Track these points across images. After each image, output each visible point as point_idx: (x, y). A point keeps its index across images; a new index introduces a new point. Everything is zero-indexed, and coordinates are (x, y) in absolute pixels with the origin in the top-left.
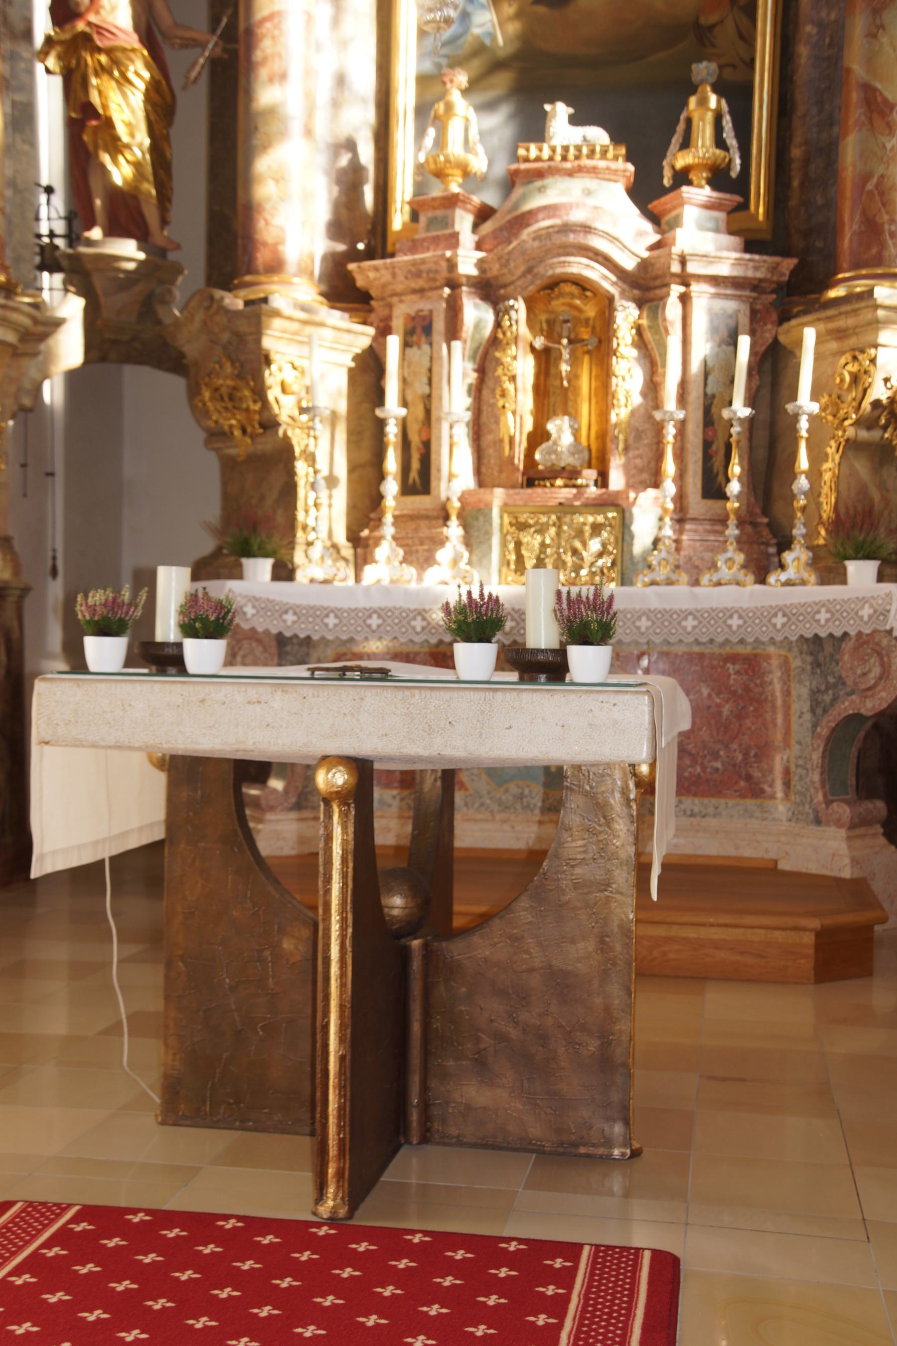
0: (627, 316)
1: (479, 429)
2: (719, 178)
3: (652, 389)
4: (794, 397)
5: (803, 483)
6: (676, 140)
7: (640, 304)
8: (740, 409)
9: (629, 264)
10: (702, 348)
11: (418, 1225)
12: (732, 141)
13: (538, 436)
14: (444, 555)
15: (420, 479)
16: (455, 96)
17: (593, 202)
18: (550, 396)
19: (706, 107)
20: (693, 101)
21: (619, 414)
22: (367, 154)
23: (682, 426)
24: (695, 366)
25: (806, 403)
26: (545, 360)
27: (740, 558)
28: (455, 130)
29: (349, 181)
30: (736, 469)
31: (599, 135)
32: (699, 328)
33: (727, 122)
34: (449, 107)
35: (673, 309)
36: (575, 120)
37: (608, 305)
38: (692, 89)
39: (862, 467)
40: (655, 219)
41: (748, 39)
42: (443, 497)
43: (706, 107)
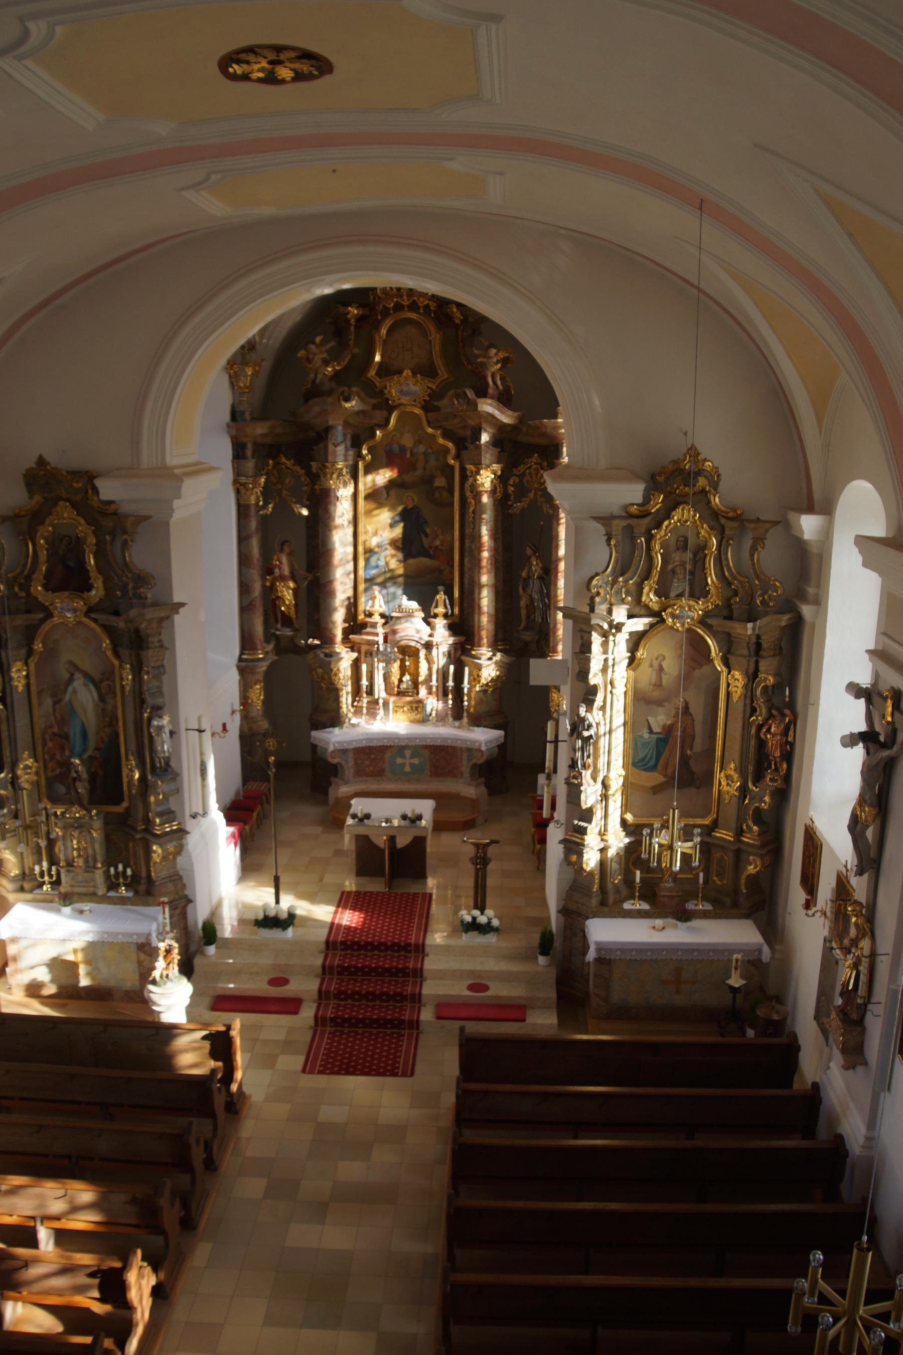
0: (422, 653)
1: (387, 677)
2: (446, 616)
3: (430, 669)
4: (462, 682)
5: (466, 703)
6: (434, 605)
7: (426, 649)
8: (451, 683)
9: (423, 642)
10: (442, 661)
11: (400, 891)
12: (449, 607)
13: (400, 681)
14: (378, 717)
15: (370, 691)
16: (377, 593)
17: (414, 629)
18: (403, 670)
19: (441, 597)
20: (438, 597)
21: (421, 679)
22: (352, 600)
23: (437, 687)
24: (440, 666)
25: (466, 685)
26: (403, 661)
27: (451, 719)
28: (377, 601)
29: (348, 608)
30: (450, 696)
31: (414, 605)
32: (440, 657)
33: (447, 601)
34: (375, 598)
35: (434, 651)
36: (409, 599)
37: (418, 650)
38: (437, 593)
39: (481, 694)
40: (428, 624)
41: (452, 573)
42: (376, 697)
43: (441, 597)
